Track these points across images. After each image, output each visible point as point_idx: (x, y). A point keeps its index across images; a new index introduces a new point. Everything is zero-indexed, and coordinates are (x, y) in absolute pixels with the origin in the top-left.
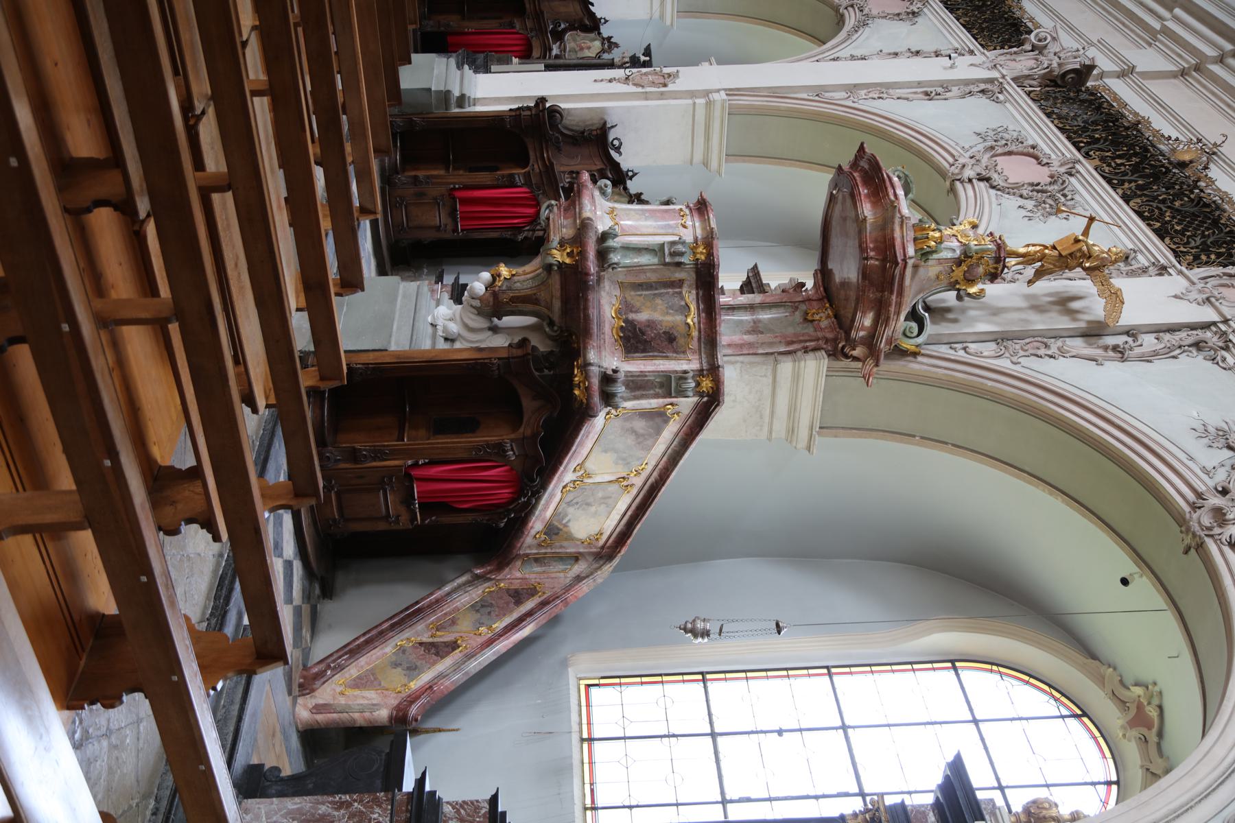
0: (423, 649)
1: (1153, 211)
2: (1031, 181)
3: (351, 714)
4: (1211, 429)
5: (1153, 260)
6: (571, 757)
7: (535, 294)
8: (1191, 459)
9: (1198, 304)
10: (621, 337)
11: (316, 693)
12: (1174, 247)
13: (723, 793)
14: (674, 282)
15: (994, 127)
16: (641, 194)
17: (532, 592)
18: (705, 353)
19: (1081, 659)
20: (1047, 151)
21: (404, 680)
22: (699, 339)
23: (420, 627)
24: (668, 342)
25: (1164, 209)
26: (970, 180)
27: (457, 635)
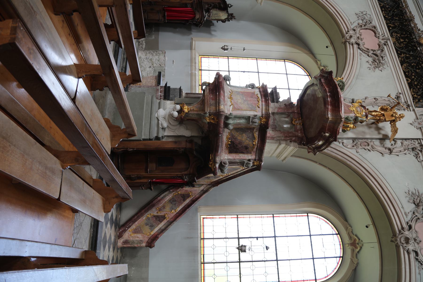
0: (155, 218)
1: (409, 72)
2: (372, 49)
3: (134, 245)
4: (410, 193)
5: (406, 101)
6: (198, 247)
7: (197, 120)
8: (403, 208)
9: (417, 129)
10: (228, 147)
11: (123, 237)
12: (413, 94)
13: (240, 259)
14: (251, 128)
15: (362, 11)
16: (233, 14)
17: (188, 196)
18: (258, 153)
19: (343, 220)
20: (379, 31)
21: (149, 231)
22: (257, 149)
23: (154, 209)
24: (245, 150)
25: (413, 71)
26: (352, 44)
27: (165, 213)
